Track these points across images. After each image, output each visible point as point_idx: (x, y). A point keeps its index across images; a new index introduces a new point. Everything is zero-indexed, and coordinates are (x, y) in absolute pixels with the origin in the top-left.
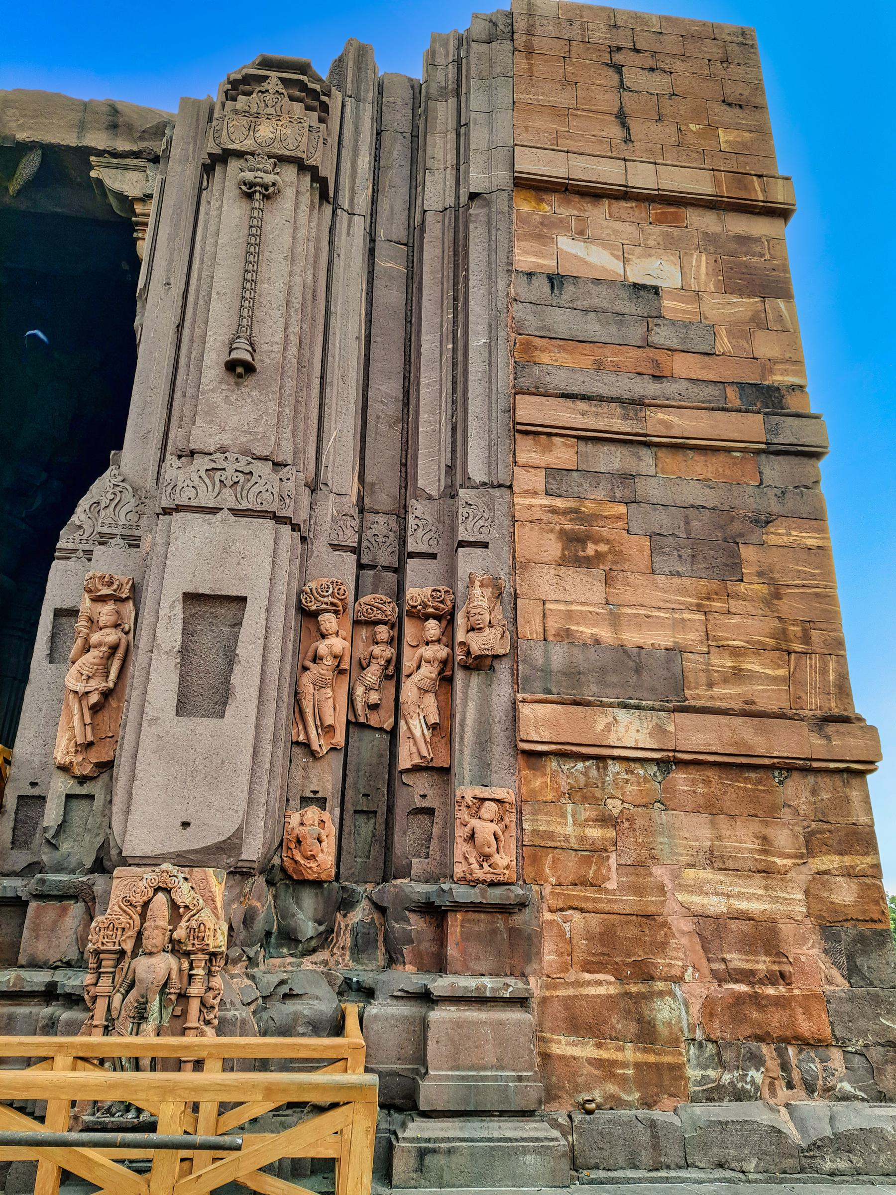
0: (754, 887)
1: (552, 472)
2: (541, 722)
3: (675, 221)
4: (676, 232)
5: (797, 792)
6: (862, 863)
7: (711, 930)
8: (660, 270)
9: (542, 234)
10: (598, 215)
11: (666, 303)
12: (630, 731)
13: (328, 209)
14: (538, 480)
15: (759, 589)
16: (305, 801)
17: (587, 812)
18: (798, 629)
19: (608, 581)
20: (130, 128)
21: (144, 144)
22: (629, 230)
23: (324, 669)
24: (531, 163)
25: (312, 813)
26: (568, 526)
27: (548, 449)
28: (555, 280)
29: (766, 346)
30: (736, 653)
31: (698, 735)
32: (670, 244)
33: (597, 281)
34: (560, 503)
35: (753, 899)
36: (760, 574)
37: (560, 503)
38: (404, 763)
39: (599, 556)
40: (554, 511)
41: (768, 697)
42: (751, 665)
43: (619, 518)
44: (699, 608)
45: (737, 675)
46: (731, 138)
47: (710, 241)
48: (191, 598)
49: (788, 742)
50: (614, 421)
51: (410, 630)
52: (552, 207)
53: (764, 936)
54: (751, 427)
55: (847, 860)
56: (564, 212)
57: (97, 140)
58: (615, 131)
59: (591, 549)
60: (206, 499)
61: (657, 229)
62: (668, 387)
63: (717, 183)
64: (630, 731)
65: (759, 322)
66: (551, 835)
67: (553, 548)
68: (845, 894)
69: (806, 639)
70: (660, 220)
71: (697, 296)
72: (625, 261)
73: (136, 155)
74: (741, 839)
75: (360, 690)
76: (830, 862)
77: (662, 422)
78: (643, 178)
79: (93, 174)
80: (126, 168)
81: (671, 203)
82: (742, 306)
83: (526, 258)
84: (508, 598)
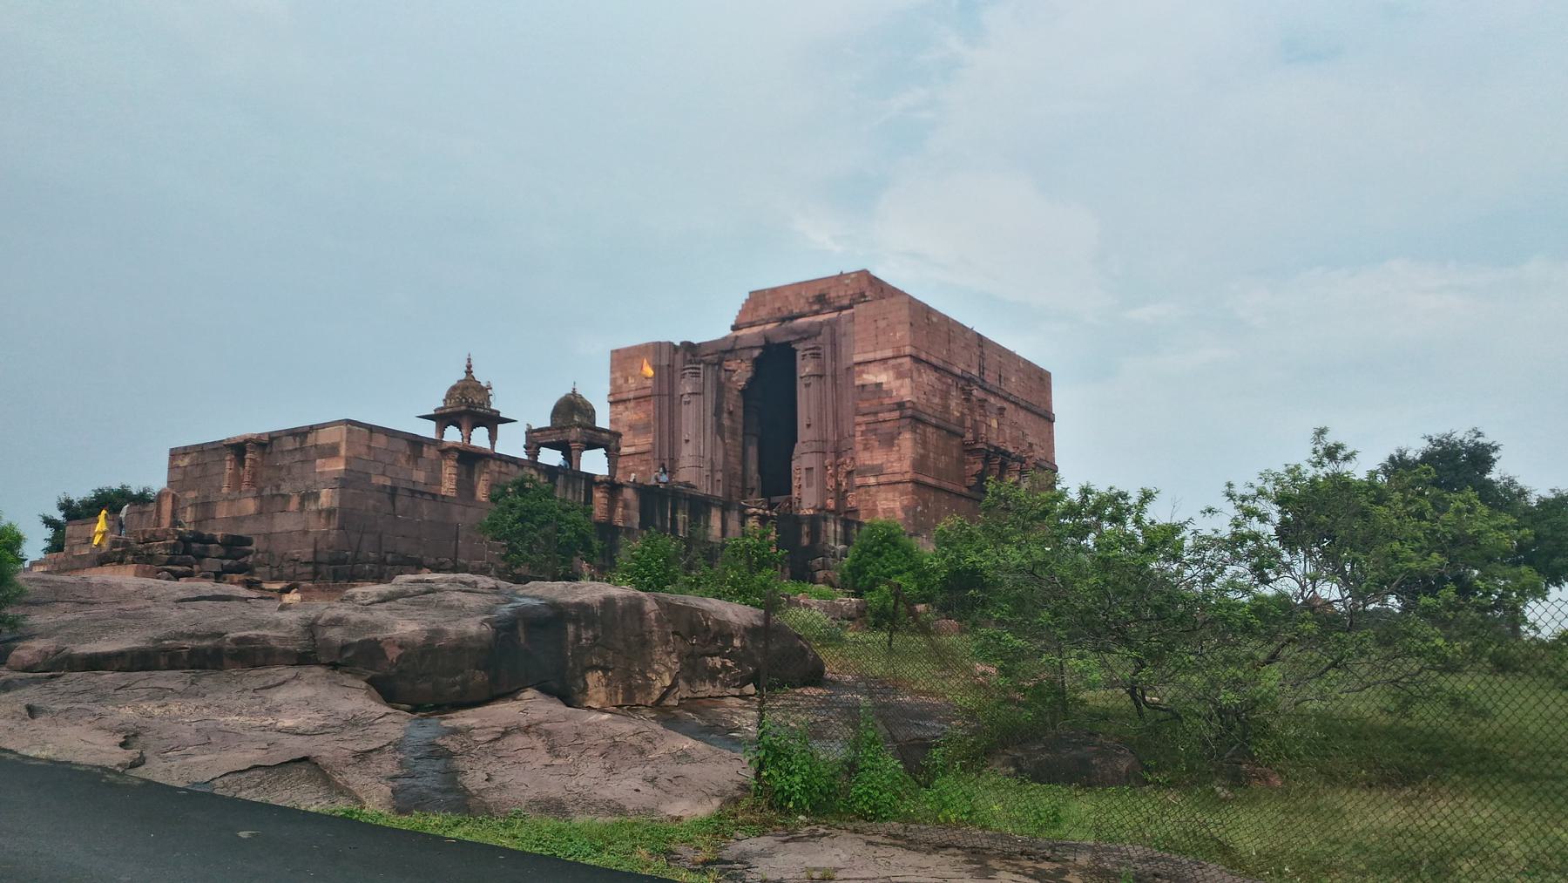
2: (858, 481)
7: (884, 511)
12: (872, 481)
24: (857, 358)
31: (882, 479)
41: (897, 470)
47: (894, 367)
53: (892, 510)
54: (896, 414)
57: (791, 338)
64: (872, 481)
74: (890, 496)
78: (879, 355)
81: (884, 360)
82: (898, 383)
83: (858, 382)
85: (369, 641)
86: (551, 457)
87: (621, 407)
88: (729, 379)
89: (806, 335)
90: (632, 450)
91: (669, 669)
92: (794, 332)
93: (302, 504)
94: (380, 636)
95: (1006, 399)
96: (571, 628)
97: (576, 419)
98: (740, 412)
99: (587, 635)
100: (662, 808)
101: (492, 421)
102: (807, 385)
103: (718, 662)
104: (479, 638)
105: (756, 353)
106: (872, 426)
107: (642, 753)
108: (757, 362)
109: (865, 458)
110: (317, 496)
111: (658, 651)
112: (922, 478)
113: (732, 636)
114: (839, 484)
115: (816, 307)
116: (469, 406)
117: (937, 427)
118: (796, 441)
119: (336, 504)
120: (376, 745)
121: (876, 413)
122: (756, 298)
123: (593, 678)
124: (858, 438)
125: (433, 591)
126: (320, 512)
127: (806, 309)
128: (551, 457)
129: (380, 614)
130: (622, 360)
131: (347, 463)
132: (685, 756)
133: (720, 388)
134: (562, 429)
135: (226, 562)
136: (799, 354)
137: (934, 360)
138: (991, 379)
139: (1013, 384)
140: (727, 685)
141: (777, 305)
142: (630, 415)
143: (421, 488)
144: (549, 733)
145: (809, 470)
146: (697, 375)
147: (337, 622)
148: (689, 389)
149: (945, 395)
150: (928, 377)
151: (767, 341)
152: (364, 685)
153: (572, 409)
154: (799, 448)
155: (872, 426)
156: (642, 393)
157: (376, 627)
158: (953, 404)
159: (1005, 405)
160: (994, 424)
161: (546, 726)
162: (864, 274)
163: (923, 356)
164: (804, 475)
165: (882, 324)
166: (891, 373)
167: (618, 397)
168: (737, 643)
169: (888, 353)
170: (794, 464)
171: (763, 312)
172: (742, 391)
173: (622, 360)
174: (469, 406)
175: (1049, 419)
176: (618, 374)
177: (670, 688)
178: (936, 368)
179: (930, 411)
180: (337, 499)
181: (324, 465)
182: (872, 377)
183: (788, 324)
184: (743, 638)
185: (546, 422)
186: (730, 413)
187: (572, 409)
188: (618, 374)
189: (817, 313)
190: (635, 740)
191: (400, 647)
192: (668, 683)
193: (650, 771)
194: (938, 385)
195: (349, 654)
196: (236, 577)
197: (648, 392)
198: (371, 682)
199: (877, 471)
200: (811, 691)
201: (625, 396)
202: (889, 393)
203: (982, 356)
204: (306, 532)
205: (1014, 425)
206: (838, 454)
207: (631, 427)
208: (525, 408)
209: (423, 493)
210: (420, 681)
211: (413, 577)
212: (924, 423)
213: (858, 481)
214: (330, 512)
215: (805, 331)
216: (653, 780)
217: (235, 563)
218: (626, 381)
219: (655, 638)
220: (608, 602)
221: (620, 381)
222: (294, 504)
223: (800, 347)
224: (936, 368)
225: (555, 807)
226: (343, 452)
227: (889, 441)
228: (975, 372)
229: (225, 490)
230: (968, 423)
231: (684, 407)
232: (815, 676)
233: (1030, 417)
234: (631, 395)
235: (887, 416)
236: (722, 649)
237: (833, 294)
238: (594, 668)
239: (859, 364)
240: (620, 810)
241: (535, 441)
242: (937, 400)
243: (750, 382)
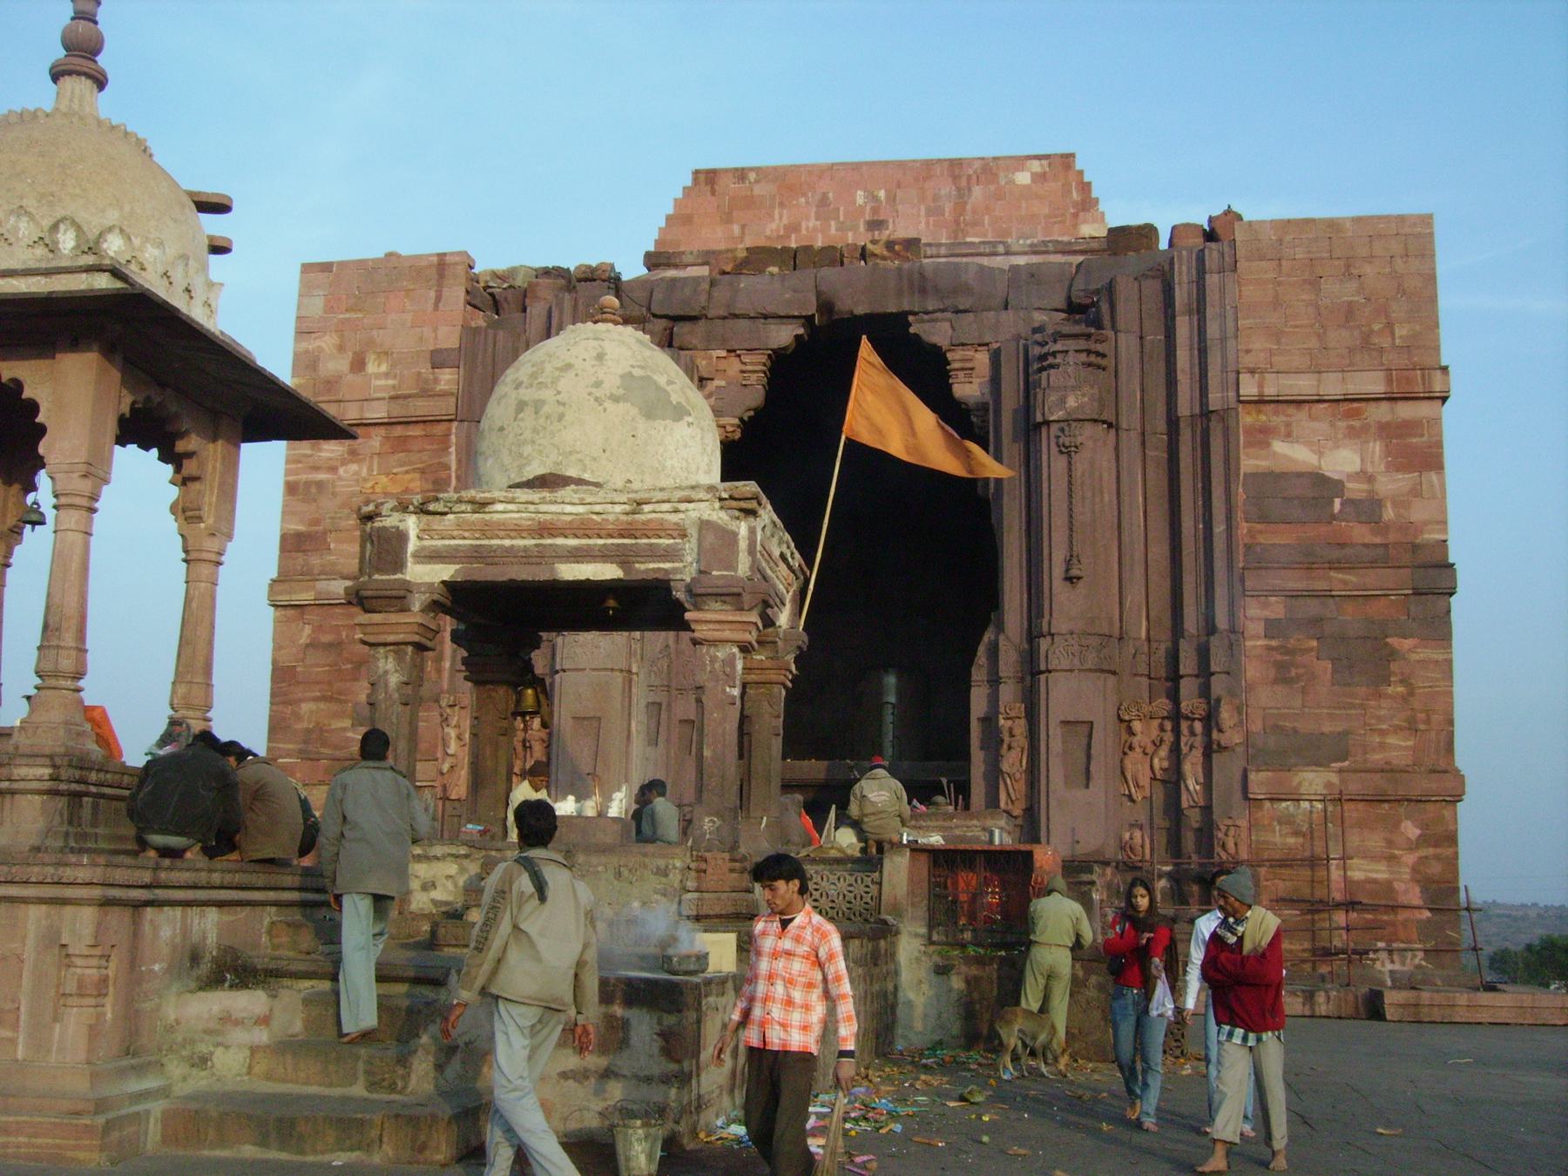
0: (1382, 866)
1: (1267, 621)
3: (1355, 414)
4: (1357, 424)
6: (1446, 851)
8: (1342, 461)
9: (1262, 436)
10: (1300, 416)
11: (1349, 485)
13: (1113, 431)
14: (1259, 628)
15: (1400, 689)
16: (1132, 826)
17: (1287, 829)
18: (1423, 715)
19: (1304, 691)
20: (937, 290)
21: (948, 302)
22: (1322, 426)
23: (1137, 754)
25: (1138, 834)
26: (1279, 658)
27: (1265, 606)
29: (1418, 513)
30: (1382, 733)
31: (1354, 786)
32: (1353, 433)
33: (1300, 475)
34: (1274, 643)
35: (1380, 872)
36: (1401, 681)
37: (1274, 643)
38: (1185, 804)
39: (1299, 677)
40: (1270, 648)
42: (1391, 740)
43: (1311, 650)
44: (1362, 706)
45: (1382, 746)
46: (1404, 332)
48: (1065, 723)
51: (1184, 725)
52: (1264, 417)
55: (1439, 851)
56: (1278, 420)
58: (1313, 343)
59: (1293, 672)
60: (1065, 664)
61: (1342, 424)
62: (1349, 551)
63: (1389, 381)
65: (1416, 492)
66: (1268, 843)
67: (1272, 673)
68: (1435, 869)
69: (1428, 721)
70: (1349, 415)
71: (1370, 479)
72: (1321, 454)
73: (943, 311)
74: (1375, 841)
75: (1156, 761)
76: (1431, 851)
77: (1341, 581)
78: (1332, 386)
79: (912, 330)
80: (936, 320)
102: (1067, 451)
105: (784, 335)
106: (1312, 608)
124: (1255, 642)
151: (826, 306)
155: (1312, 608)
156: (421, 407)
166: (1376, 448)
169: (1373, 383)
182: (1293, 453)
202: (1368, 509)
215: (966, 289)
218: (359, 365)
221: (337, 365)
234: (378, 412)
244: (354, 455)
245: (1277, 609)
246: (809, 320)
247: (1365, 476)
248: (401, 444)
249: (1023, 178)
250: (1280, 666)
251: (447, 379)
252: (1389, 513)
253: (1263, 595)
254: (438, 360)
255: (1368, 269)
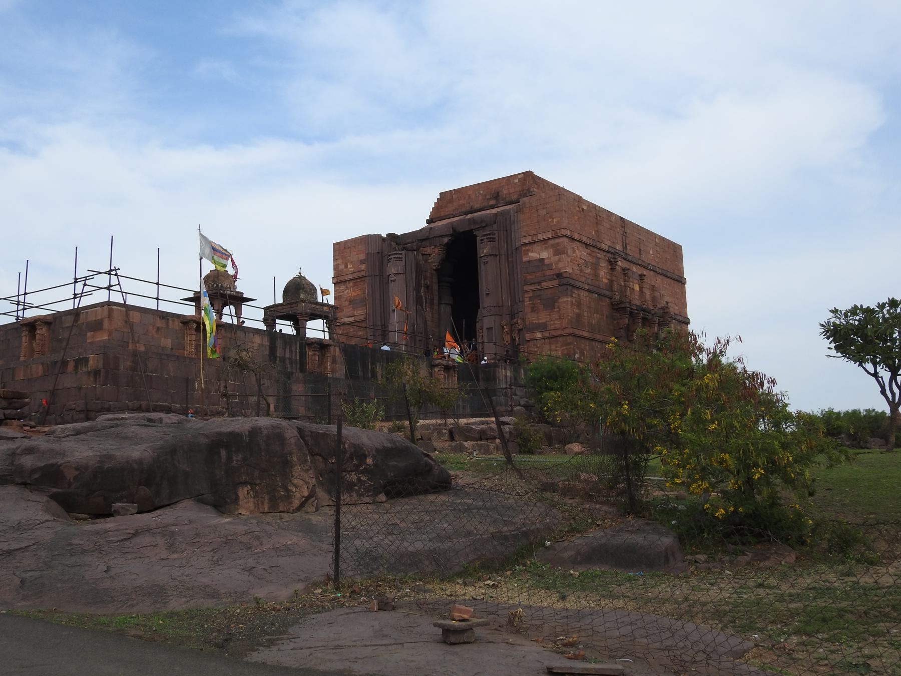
2: (528, 336)
5: (561, 339)
8: (544, 255)
10: (535, 246)
12: (539, 335)
24: (524, 241)
28: (529, 262)
31: (546, 334)
32: (546, 248)
41: (558, 326)
49: (559, 333)
50: (537, 287)
54: (555, 283)
64: (539, 335)
65: (559, 261)
81: (545, 241)
82: (557, 258)
83: (525, 259)
84: (523, 320)
85: (52, 465)
86: (285, 327)
87: (343, 287)
88: (426, 261)
89: (483, 224)
90: (352, 319)
91: (307, 483)
92: (473, 221)
93: (76, 367)
94: (59, 461)
95: (646, 268)
96: (223, 453)
97: (302, 296)
98: (436, 287)
99: (237, 458)
100: (252, 591)
101: (239, 300)
103: (354, 478)
104: (140, 462)
105: (446, 240)
106: (538, 293)
107: (249, 548)
108: (448, 248)
109: (532, 318)
110: (86, 360)
111: (297, 471)
112: (577, 332)
113: (365, 456)
114: (513, 340)
115: (492, 202)
116: (221, 290)
117: (589, 291)
118: (479, 307)
119: (100, 365)
120: (23, 545)
121: (540, 283)
122: (445, 199)
123: (243, 492)
125: (117, 426)
126: (89, 373)
127: (485, 204)
128: (285, 327)
129: (68, 444)
130: (341, 250)
131: (110, 334)
132: (288, 550)
133: (419, 270)
134: (291, 304)
135: (8, 412)
136: (478, 239)
137: (585, 239)
138: (632, 251)
139: (650, 255)
140: (362, 495)
141: (461, 202)
142: (349, 292)
143: (169, 352)
144: (172, 533)
145: (490, 329)
146: (400, 259)
147: (30, 451)
148: (393, 271)
149: (595, 267)
150: (582, 253)
151: (454, 230)
152: (45, 499)
153: (298, 289)
154: (482, 312)
157: (63, 454)
158: (602, 273)
159: (645, 272)
160: (637, 288)
161: (172, 528)
162: (529, 175)
163: (576, 236)
164: (485, 331)
165: (542, 212)
166: (551, 250)
167: (341, 279)
168: (369, 461)
169: (549, 235)
170: (478, 326)
171: (450, 208)
172: (436, 270)
173: (341, 250)
174: (221, 290)
175: (681, 282)
176: (339, 262)
177: (308, 498)
178: (587, 245)
179: (583, 279)
180: (101, 362)
181: (93, 337)
182: (533, 255)
183: (469, 216)
184: (374, 457)
185: (280, 300)
186: (427, 287)
187: (298, 289)
188: (339, 262)
189: (493, 207)
190: (244, 539)
191: (76, 469)
192: (306, 494)
193: (251, 562)
194: (589, 259)
195: (36, 476)
196: (15, 422)
197: (363, 274)
198: (54, 497)
199: (543, 327)
200: (443, 498)
201: (345, 278)
203: (624, 234)
204: (80, 389)
205: (653, 288)
206: (512, 315)
207: (351, 302)
208: (261, 288)
209: (167, 355)
210: (88, 495)
211: (110, 416)
212: (578, 288)
213: (528, 336)
214: (96, 373)
215: (482, 221)
216: (250, 570)
217: (14, 411)
218: (346, 266)
219: (295, 459)
220: (254, 432)
221: (342, 267)
222: (71, 367)
223: (479, 234)
224: (587, 245)
225: (158, 593)
226: (106, 324)
227: (551, 304)
228: (619, 247)
229: (22, 359)
230: (615, 287)
231: (391, 285)
232: (443, 484)
233: (666, 280)
234: (350, 277)
235: (546, 284)
236: (357, 466)
237: (505, 192)
238: (245, 483)
239: (526, 244)
240: (214, 594)
241: (272, 314)
242: (588, 271)
243: (444, 262)
244: (347, 288)
245: (531, 294)
246: (451, 235)
247: (549, 258)
248: (355, 284)
249: (517, 181)
250: (533, 308)
251: (363, 267)
252: (554, 267)
253: (527, 292)
254: (362, 262)
255: (548, 206)
